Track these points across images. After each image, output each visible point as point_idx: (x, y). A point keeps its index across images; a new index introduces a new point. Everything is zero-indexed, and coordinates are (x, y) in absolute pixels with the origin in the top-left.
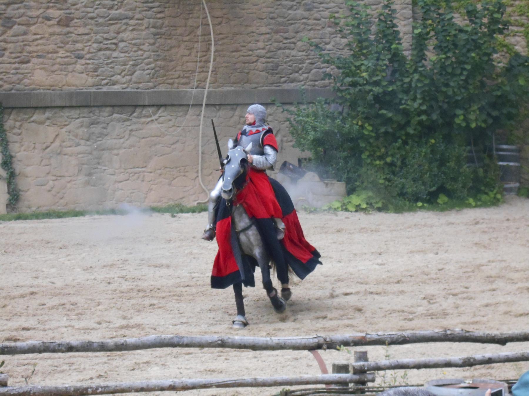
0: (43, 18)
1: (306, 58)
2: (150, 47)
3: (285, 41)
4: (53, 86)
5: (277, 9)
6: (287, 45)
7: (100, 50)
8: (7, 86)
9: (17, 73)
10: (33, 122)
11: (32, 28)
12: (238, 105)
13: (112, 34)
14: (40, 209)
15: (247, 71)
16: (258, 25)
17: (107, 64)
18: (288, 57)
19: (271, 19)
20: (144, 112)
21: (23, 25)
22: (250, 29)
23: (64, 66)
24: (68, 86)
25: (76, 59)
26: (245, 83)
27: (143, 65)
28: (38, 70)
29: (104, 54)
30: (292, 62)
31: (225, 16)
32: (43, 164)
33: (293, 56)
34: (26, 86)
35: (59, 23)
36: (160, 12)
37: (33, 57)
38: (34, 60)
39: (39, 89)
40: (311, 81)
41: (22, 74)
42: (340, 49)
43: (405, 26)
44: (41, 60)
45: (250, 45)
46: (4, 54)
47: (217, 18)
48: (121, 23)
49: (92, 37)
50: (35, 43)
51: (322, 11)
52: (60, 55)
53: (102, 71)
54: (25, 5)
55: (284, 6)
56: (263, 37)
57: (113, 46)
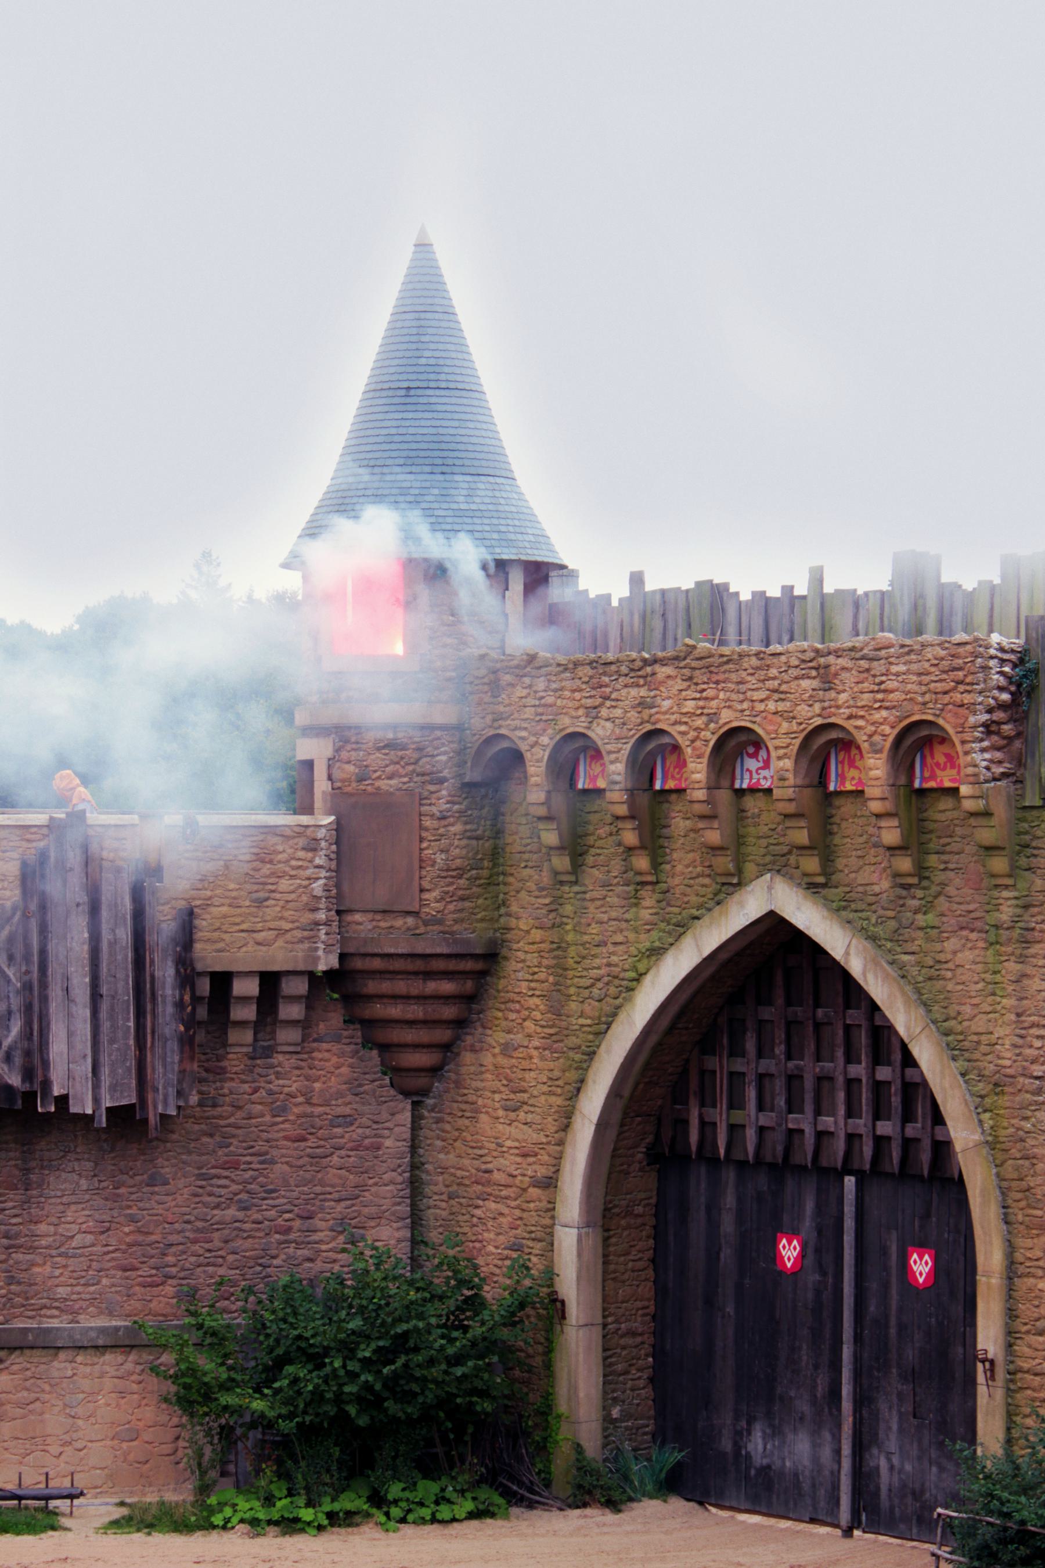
3: (208, 1255)
5: (195, 1208)
12: (132, 1347)
15: (149, 1298)
18: (212, 1277)
36: (16, 1216)
43: (398, 1229)
51: (266, 1210)
55: (205, 1205)
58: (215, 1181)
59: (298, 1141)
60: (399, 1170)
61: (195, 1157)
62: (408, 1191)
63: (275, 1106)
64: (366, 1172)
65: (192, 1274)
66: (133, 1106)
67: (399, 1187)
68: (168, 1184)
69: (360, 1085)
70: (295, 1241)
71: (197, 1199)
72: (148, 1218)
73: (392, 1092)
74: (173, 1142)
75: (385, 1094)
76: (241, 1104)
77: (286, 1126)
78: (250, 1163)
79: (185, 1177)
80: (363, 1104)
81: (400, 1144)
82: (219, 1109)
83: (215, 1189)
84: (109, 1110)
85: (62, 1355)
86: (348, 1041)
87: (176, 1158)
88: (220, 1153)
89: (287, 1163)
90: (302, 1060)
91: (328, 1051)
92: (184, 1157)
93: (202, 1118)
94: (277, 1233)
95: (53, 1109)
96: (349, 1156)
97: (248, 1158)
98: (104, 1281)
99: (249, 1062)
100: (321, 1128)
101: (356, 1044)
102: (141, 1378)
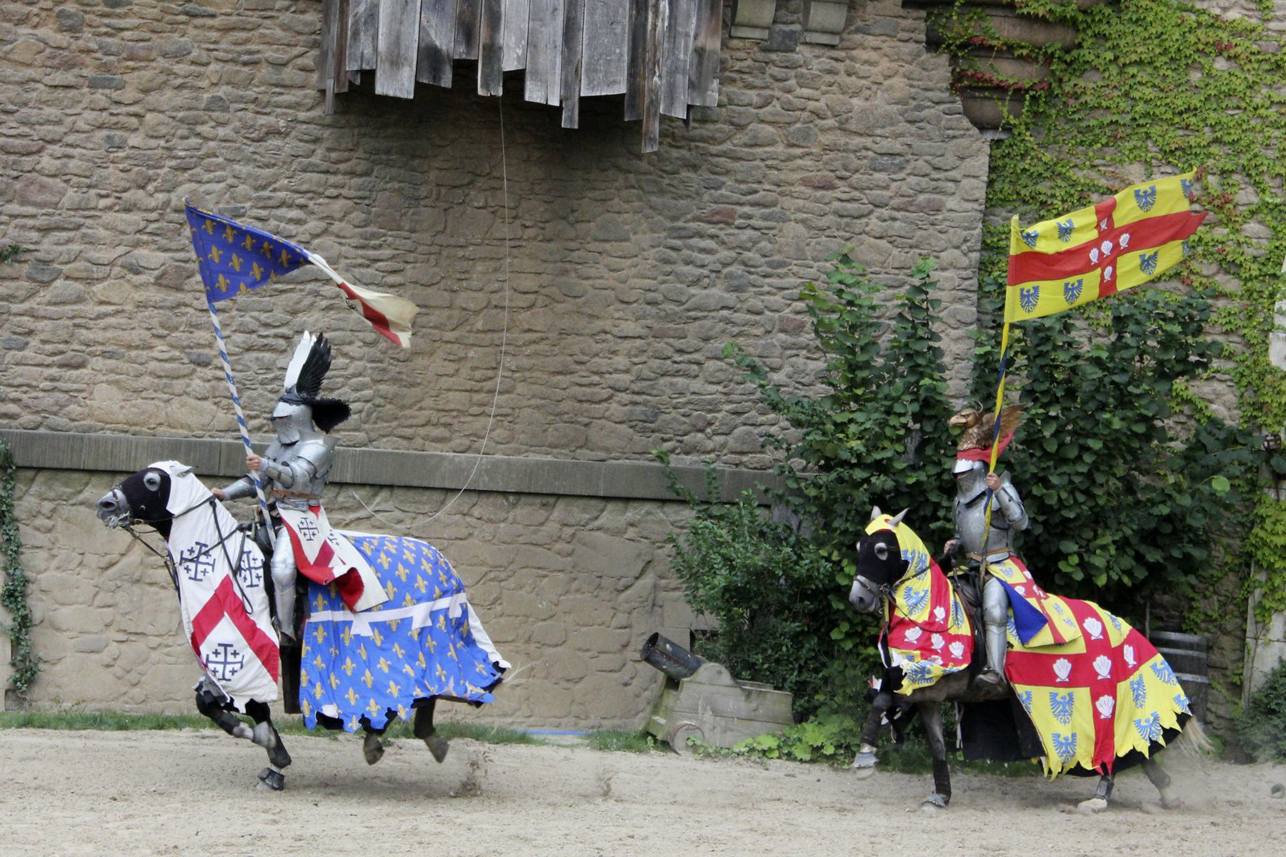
0: (122, 266)
1: (724, 398)
2: (366, 349)
3: (678, 358)
4: (136, 425)
5: (664, 282)
6: (682, 366)
7: (249, 350)
8: (27, 418)
9: (54, 389)
10: (82, 503)
11: (97, 288)
12: (559, 496)
13: (279, 315)
14: (83, 705)
15: (587, 420)
16: (617, 315)
17: (262, 383)
18: (682, 394)
19: (649, 304)
20: (340, 499)
21: (76, 279)
22: (598, 325)
23: (165, 380)
24: (169, 426)
25: (192, 366)
26: (581, 447)
27: (346, 389)
28: (104, 385)
29: (257, 359)
30: (691, 407)
31: (543, 291)
32: (96, 603)
33: (694, 393)
34: (73, 420)
35: (158, 282)
36: (394, 272)
37: (93, 355)
38: (98, 363)
39: (103, 429)
40: (732, 453)
41: (66, 392)
42: (804, 385)
43: (957, 340)
44: (111, 363)
45: (596, 359)
46: (27, 343)
47: (525, 293)
48: (301, 290)
49: (233, 318)
50: (102, 323)
51: (769, 293)
52: (155, 354)
53: (249, 398)
54: (84, 235)
55: (680, 277)
56: (627, 344)
57: (282, 342)
58: (695, 241)
59: (823, 188)
60: (964, 247)
61: (667, 200)
62: (975, 281)
63: (792, 129)
64: (917, 247)
65: (652, 387)
66: (623, 96)
67: (964, 274)
68: (627, 240)
69: (919, 108)
70: (806, 347)
71: (668, 268)
72: (591, 291)
73: (966, 123)
74: (638, 172)
75: (954, 124)
76: (743, 122)
77: (807, 162)
78: (750, 217)
79: (653, 231)
80: (920, 136)
81: (969, 206)
82: (710, 126)
83: (696, 254)
84: (587, 104)
85: (453, 501)
86: (906, 35)
87: (640, 199)
88: (706, 197)
89: (803, 221)
90: (836, 60)
91: (876, 49)
92: (653, 198)
93: (683, 138)
94: (783, 331)
95: (501, 94)
96: (894, 219)
97: (747, 209)
98: (521, 388)
99: (760, 56)
100: (857, 171)
101: (917, 42)
102: (570, 547)
